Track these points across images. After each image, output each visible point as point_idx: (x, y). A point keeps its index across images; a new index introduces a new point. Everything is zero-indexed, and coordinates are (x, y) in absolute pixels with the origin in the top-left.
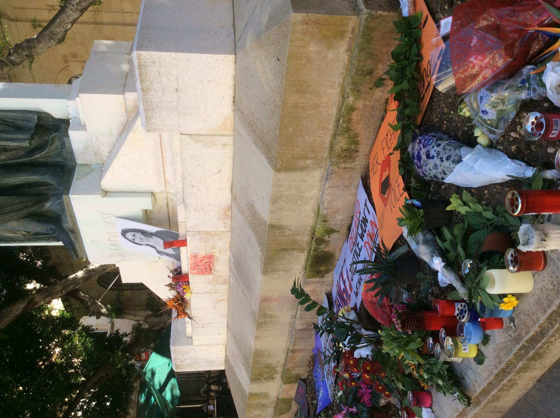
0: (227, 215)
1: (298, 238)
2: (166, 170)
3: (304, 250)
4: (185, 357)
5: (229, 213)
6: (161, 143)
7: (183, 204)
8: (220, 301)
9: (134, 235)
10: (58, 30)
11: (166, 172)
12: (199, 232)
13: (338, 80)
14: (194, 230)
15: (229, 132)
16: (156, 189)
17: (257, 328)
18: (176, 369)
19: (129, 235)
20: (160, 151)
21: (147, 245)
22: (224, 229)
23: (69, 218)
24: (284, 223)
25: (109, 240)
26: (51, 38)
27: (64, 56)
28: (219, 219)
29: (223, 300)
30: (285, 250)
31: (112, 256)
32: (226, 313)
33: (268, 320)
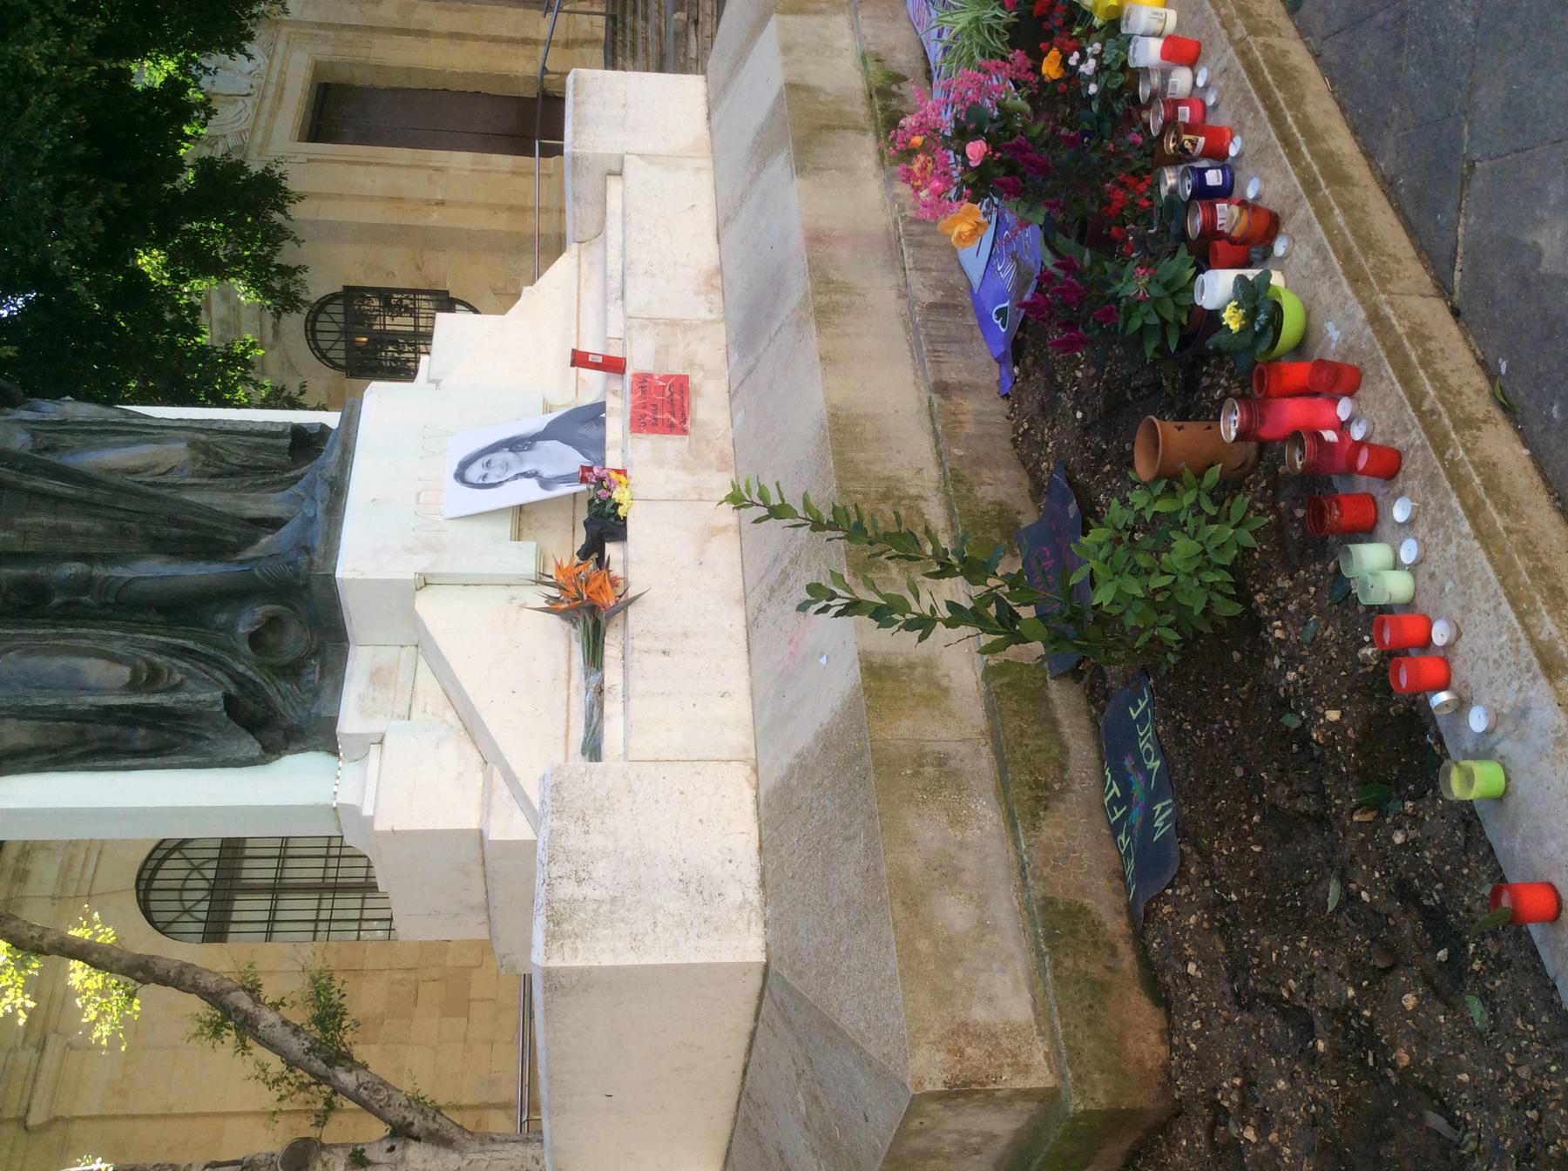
1: (847, 108)
4: (597, 841)
5: (717, 281)
7: (619, 302)
8: (715, 531)
12: (654, 321)
14: (643, 315)
18: (551, 937)
19: (474, 473)
21: (516, 477)
24: (812, 80)
28: (697, 293)
29: (724, 529)
30: (830, 128)
31: (409, 550)
33: (839, 297)
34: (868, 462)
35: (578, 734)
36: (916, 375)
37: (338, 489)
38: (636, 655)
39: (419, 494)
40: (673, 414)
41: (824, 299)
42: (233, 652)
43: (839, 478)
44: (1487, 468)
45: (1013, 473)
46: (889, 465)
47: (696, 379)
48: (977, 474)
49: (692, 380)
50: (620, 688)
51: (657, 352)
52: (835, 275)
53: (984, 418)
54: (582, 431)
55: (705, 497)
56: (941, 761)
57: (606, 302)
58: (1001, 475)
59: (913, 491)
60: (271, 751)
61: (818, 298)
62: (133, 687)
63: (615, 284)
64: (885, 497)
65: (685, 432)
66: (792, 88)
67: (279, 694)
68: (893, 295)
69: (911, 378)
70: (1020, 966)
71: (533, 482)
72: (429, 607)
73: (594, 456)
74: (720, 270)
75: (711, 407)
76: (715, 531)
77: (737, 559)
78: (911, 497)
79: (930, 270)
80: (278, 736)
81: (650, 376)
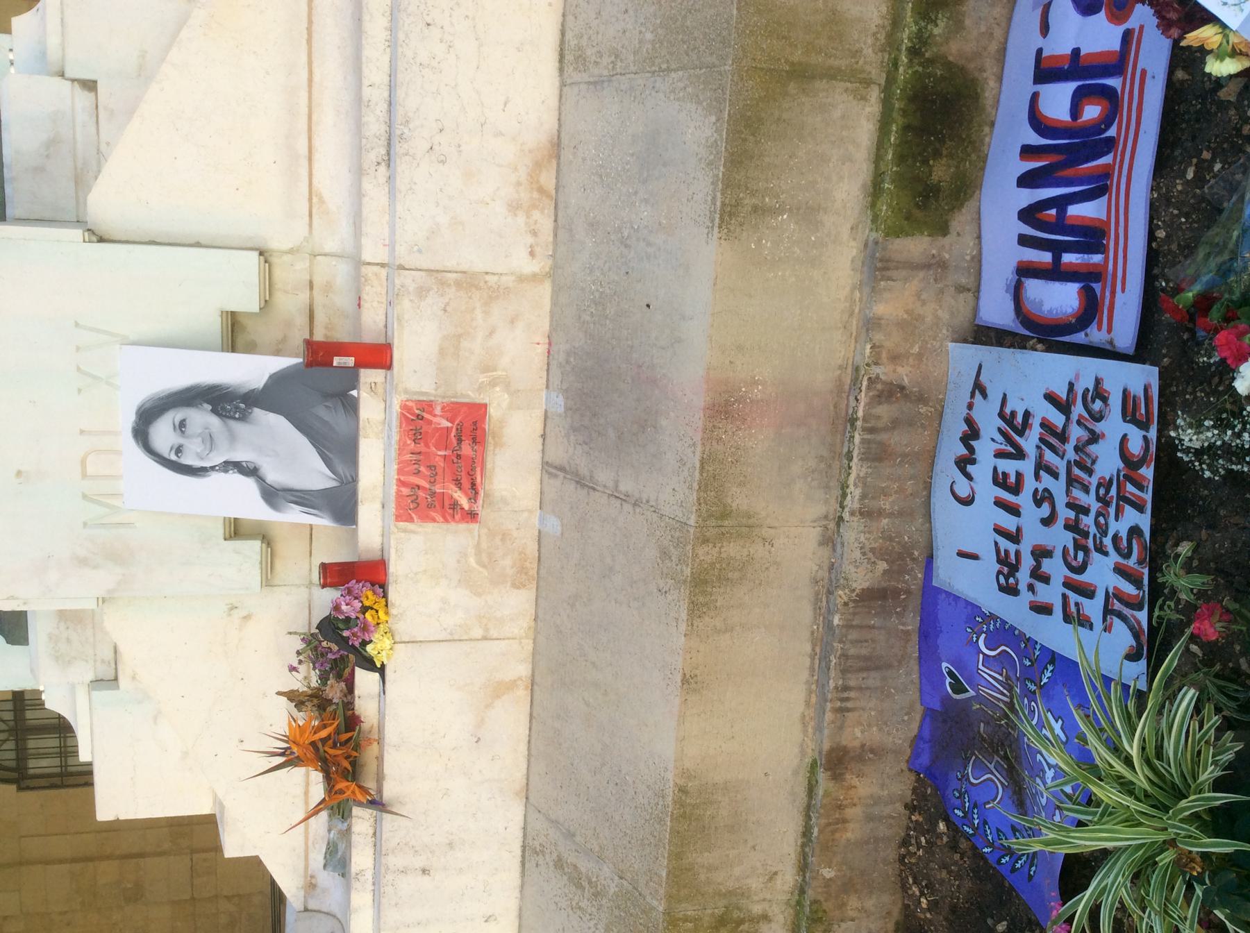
0: (541, 190)
2: (317, 143)
3: (867, 83)
5: (548, 179)
6: (310, 22)
8: (500, 689)
9: (182, 424)
11: (317, 156)
16: (277, 242)
17: (696, 610)
19: (163, 434)
20: (304, 58)
21: (228, 466)
25: (84, 475)
28: (514, 207)
29: (512, 685)
30: (803, 75)
31: (83, 562)
33: (732, 549)
34: (711, 868)
36: (808, 703)
38: (390, 877)
39: (83, 463)
40: (458, 484)
41: (707, 554)
43: (669, 897)
45: (886, 898)
46: (737, 871)
47: (498, 406)
48: (843, 905)
49: (493, 411)
50: (369, 875)
51: (442, 352)
52: (738, 499)
53: (876, 811)
54: (321, 411)
55: (494, 633)
57: (359, 172)
58: (870, 903)
59: (757, 909)
61: (701, 551)
63: (375, 126)
65: (472, 516)
68: (814, 534)
69: (800, 708)
71: (250, 484)
73: (340, 469)
74: (556, 147)
75: (513, 473)
76: (500, 689)
77: (524, 731)
78: (752, 920)
79: (880, 513)
81: (427, 406)
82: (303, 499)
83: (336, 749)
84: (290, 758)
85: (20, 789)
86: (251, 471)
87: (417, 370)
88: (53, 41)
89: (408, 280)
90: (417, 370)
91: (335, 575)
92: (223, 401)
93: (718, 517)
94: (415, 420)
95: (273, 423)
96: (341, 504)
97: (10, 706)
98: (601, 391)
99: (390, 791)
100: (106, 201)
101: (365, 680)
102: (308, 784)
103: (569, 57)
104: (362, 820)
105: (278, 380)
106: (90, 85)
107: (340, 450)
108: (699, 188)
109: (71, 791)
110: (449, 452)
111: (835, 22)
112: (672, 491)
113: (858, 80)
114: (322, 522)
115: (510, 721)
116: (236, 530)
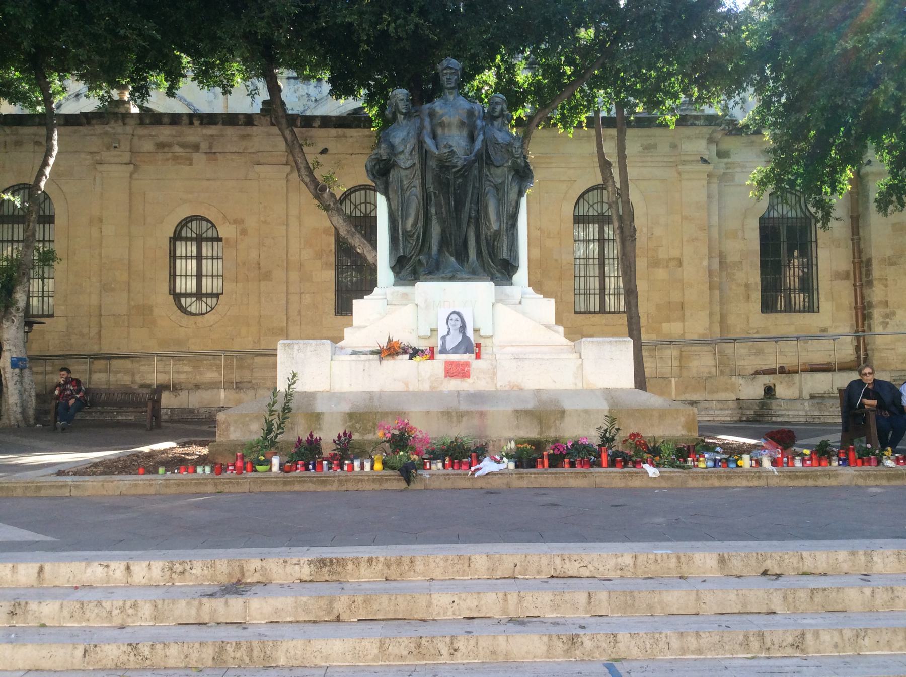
5: (515, 388)
8: (407, 384)
10: (357, 240)
13: (667, 433)
15: (585, 387)
16: (494, 339)
17: (442, 412)
18: (285, 344)
19: (454, 317)
22: (498, 386)
23: (467, 276)
26: (348, 232)
27: (242, 221)
28: (509, 382)
30: (540, 423)
31: (426, 301)
32: (386, 390)
33: (455, 419)
35: (357, 349)
37: (452, 278)
41: (454, 414)
42: (418, 255)
44: (206, 484)
47: (470, 381)
49: (468, 380)
52: (465, 419)
56: (292, 428)
60: (393, 268)
62: (405, 232)
64: (375, 424)
65: (446, 377)
66: (563, 412)
67: (408, 269)
70: (241, 438)
72: (410, 307)
75: (455, 385)
76: (407, 384)
80: (397, 270)
82: (444, 344)
83: (391, 350)
84: (390, 341)
85: (170, 238)
86: (449, 333)
87: (476, 364)
88: (528, 296)
89: (494, 362)
90: (476, 365)
91: (432, 350)
92: (463, 328)
93: (461, 415)
94: (467, 364)
95: (459, 338)
96: (443, 351)
97: (215, 235)
98: (478, 397)
99: (384, 362)
100: (500, 306)
101: (407, 356)
102: (384, 343)
103: (538, 391)
104: (376, 357)
105: (469, 339)
106: (520, 303)
107: (455, 350)
108: (520, 407)
109: (168, 260)
110: (457, 371)
111: (549, 427)
112: (464, 407)
113: (541, 433)
114: (439, 348)
115: (399, 387)
116: (434, 331)
